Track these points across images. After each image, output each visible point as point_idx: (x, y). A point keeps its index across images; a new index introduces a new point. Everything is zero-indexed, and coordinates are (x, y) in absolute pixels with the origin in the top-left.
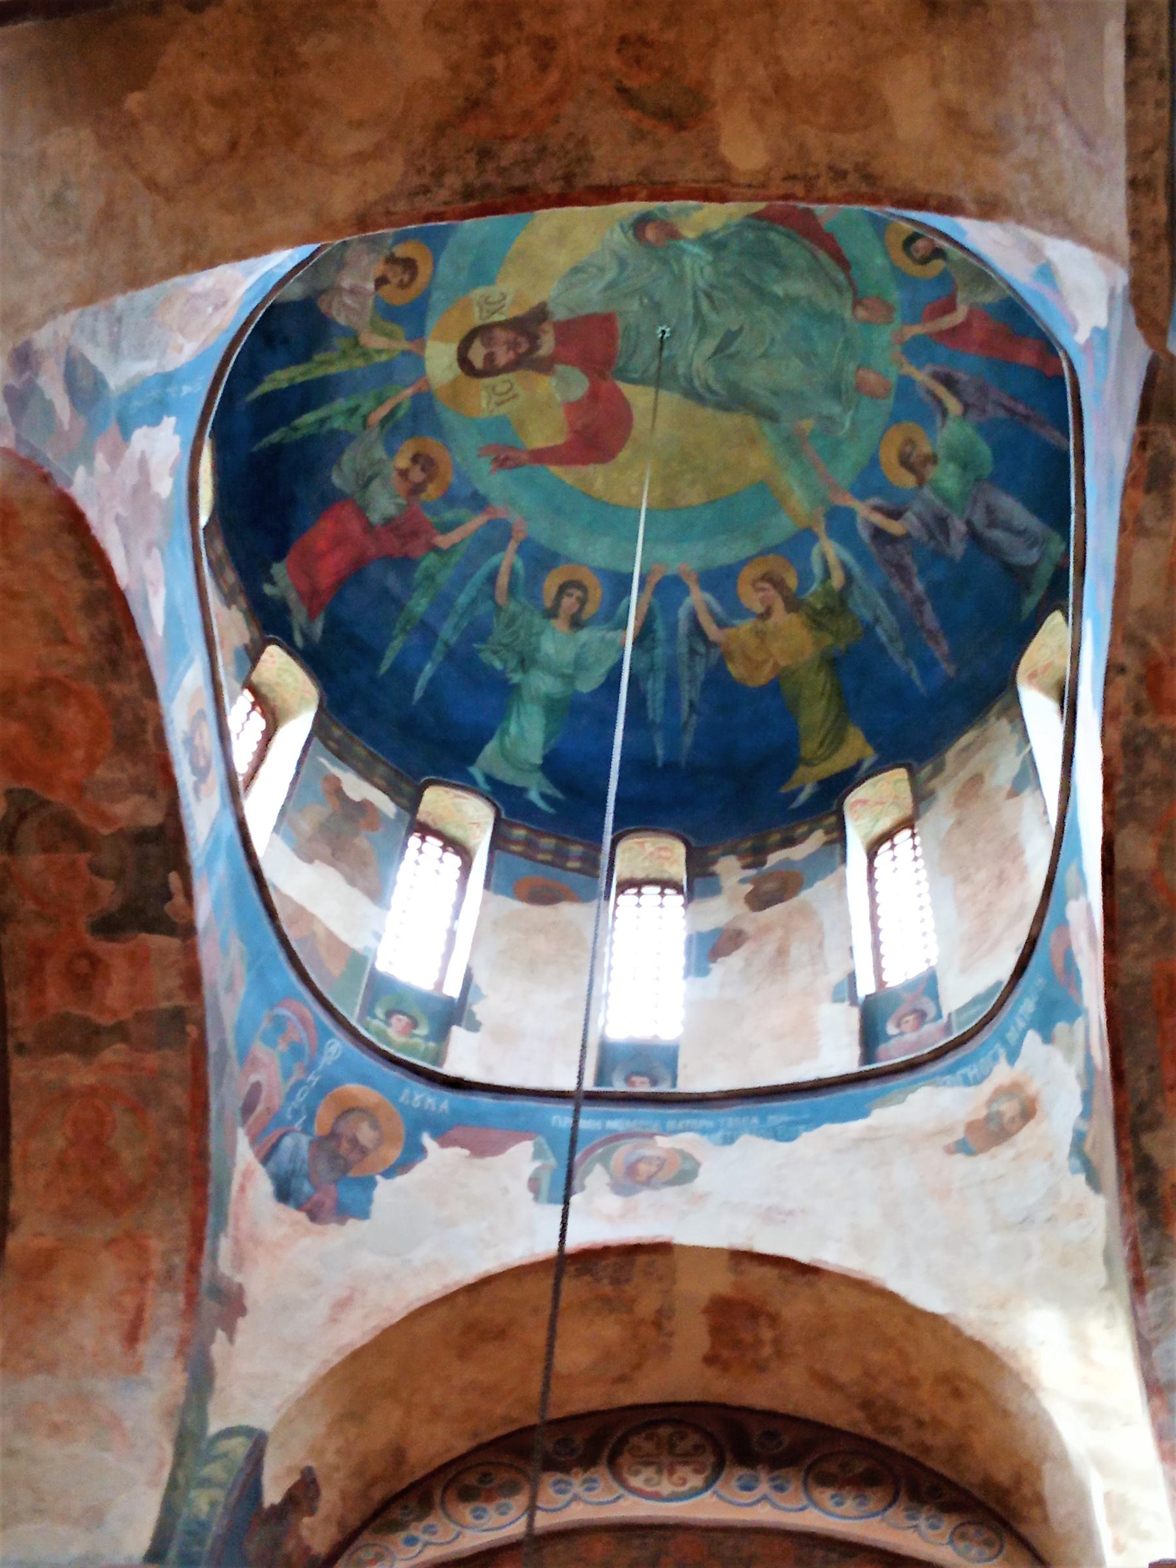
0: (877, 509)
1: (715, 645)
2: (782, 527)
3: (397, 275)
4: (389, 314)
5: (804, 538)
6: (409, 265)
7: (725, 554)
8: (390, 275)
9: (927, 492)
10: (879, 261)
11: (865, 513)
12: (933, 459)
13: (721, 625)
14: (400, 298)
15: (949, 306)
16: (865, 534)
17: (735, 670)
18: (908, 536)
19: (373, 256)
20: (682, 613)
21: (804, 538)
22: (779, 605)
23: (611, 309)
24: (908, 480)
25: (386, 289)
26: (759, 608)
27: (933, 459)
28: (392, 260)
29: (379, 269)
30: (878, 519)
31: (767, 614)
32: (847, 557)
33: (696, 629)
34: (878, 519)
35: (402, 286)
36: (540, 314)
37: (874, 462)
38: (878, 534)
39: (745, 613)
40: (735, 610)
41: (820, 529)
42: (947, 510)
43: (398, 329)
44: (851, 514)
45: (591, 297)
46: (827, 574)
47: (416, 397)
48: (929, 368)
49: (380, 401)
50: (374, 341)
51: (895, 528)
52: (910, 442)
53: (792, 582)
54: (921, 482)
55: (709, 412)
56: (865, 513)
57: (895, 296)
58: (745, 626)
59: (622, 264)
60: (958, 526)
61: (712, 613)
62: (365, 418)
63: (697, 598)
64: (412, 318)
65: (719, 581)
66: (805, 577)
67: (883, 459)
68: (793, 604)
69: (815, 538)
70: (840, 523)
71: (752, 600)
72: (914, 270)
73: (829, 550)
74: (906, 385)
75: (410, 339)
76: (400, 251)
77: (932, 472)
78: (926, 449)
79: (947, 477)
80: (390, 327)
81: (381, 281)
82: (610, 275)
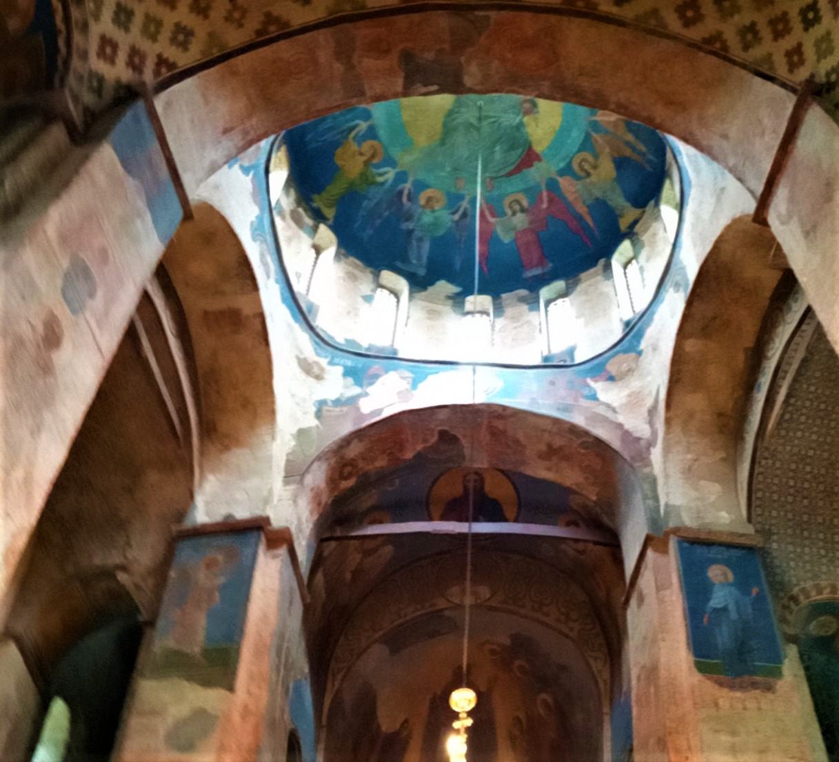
0: (409, 190)
1: (346, 138)
2: (395, 153)
5: (391, 162)
7: (382, 133)
9: (420, 210)
11: (407, 186)
12: (433, 211)
13: (354, 138)
15: (493, 215)
16: (400, 187)
17: (339, 151)
18: (402, 204)
20: (357, 121)
21: (391, 162)
22: (364, 158)
24: (422, 202)
26: (363, 151)
27: (433, 211)
30: (406, 192)
31: (361, 154)
32: (390, 182)
33: (353, 128)
34: (406, 192)
37: (428, 187)
38: (400, 193)
39: (360, 144)
40: (361, 139)
41: (397, 170)
42: (415, 219)
44: (405, 182)
46: (381, 175)
48: (468, 206)
51: (405, 199)
52: (437, 202)
53: (375, 161)
54: (424, 207)
55: (442, 119)
56: (407, 186)
58: (355, 147)
60: (410, 225)
61: (360, 131)
63: (363, 126)
65: (372, 133)
66: (378, 166)
67: (429, 190)
68: (367, 163)
69: (394, 168)
70: (401, 177)
71: (366, 146)
73: (390, 175)
74: (461, 198)
77: (428, 211)
78: (436, 208)
79: (427, 218)
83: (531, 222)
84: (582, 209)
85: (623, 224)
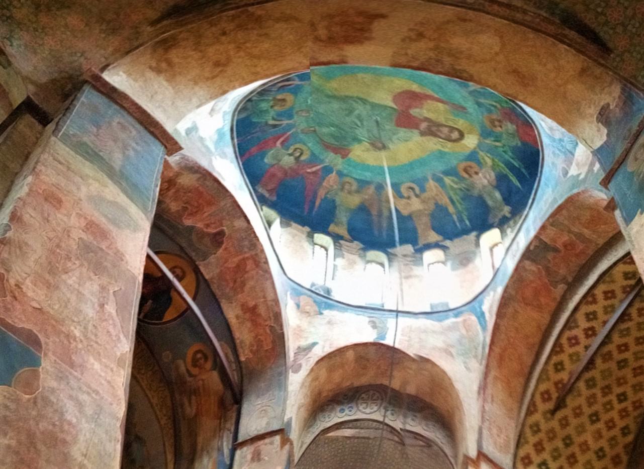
3: (472, 171)
4: (480, 164)
6: (465, 170)
8: (473, 172)
10: (310, 145)
14: (473, 164)
19: (475, 181)
23: (395, 128)
25: (476, 170)
28: (471, 176)
29: (475, 176)
35: (471, 167)
36: (423, 134)
43: (480, 158)
45: (403, 132)
47: (485, 138)
49: (496, 147)
50: (489, 162)
57: (301, 136)
59: (390, 139)
62: (504, 146)
64: (472, 156)
72: (298, 146)
75: (478, 153)
76: (466, 176)
80: (482, 161)
81: (477, 173)
82: (395, 137)
83: (290, 168)
84: (321, 193)
85: (332, 228)
